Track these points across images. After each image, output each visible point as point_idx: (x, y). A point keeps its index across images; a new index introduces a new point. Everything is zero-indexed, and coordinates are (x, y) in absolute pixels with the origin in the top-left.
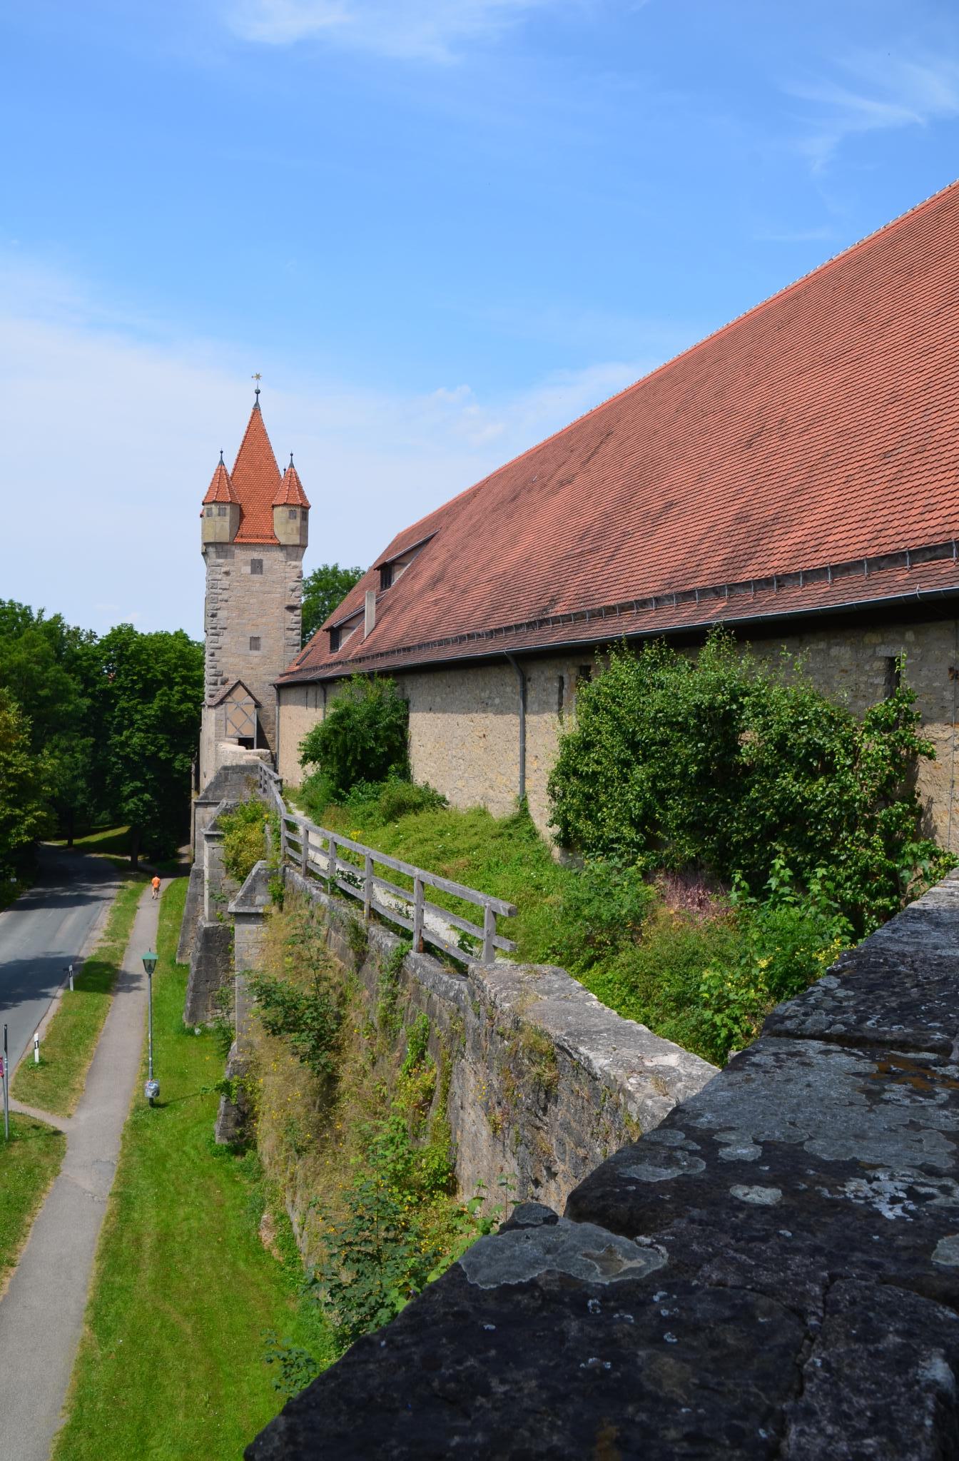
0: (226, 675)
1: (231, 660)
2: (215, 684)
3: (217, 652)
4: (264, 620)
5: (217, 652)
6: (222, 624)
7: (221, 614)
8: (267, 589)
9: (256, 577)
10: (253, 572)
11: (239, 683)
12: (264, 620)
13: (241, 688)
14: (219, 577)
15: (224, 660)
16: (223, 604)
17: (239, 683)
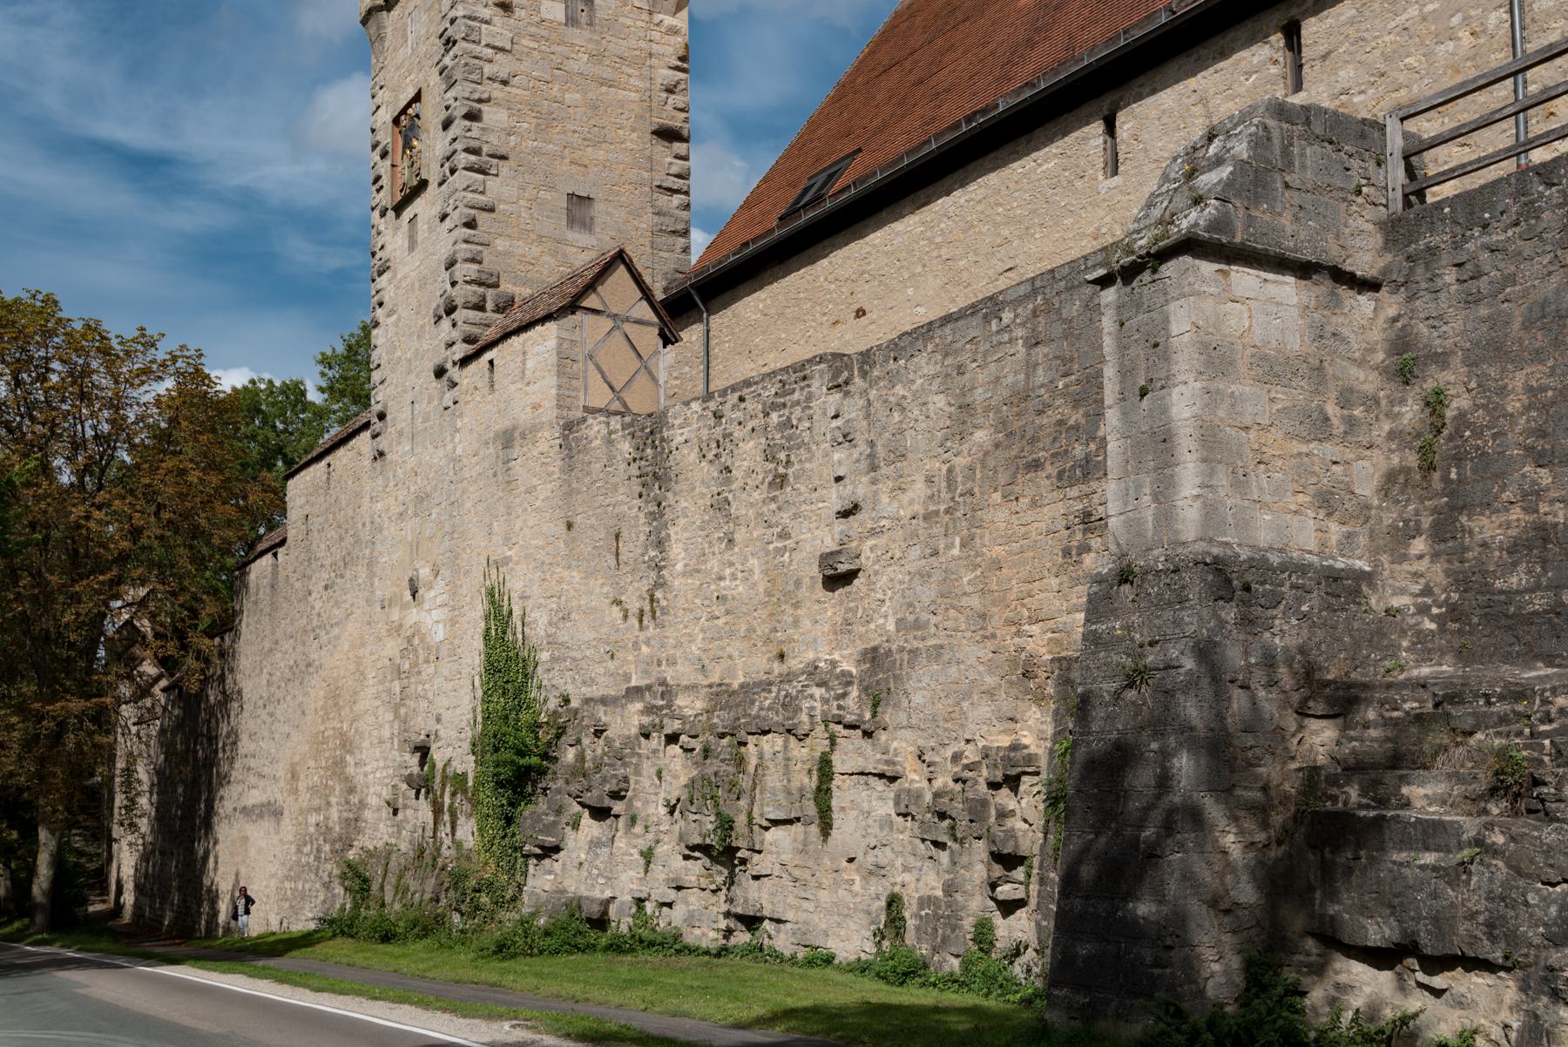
0: (506, 287)
1: (520, 247)
2: (480, 307)
3: (482, 218)
4: (601, 155)
5: (482, 218)
6: (494, 142)
7: (493, 116)
8: (607, 73)
9: (578, 36)
10: (571, 21)
11: (621, 257)
12: (601, 155)
13: (621, 272)
14: (486, 13)
15: (501, 244)
16: (496, 91)
17: (621, 257)
